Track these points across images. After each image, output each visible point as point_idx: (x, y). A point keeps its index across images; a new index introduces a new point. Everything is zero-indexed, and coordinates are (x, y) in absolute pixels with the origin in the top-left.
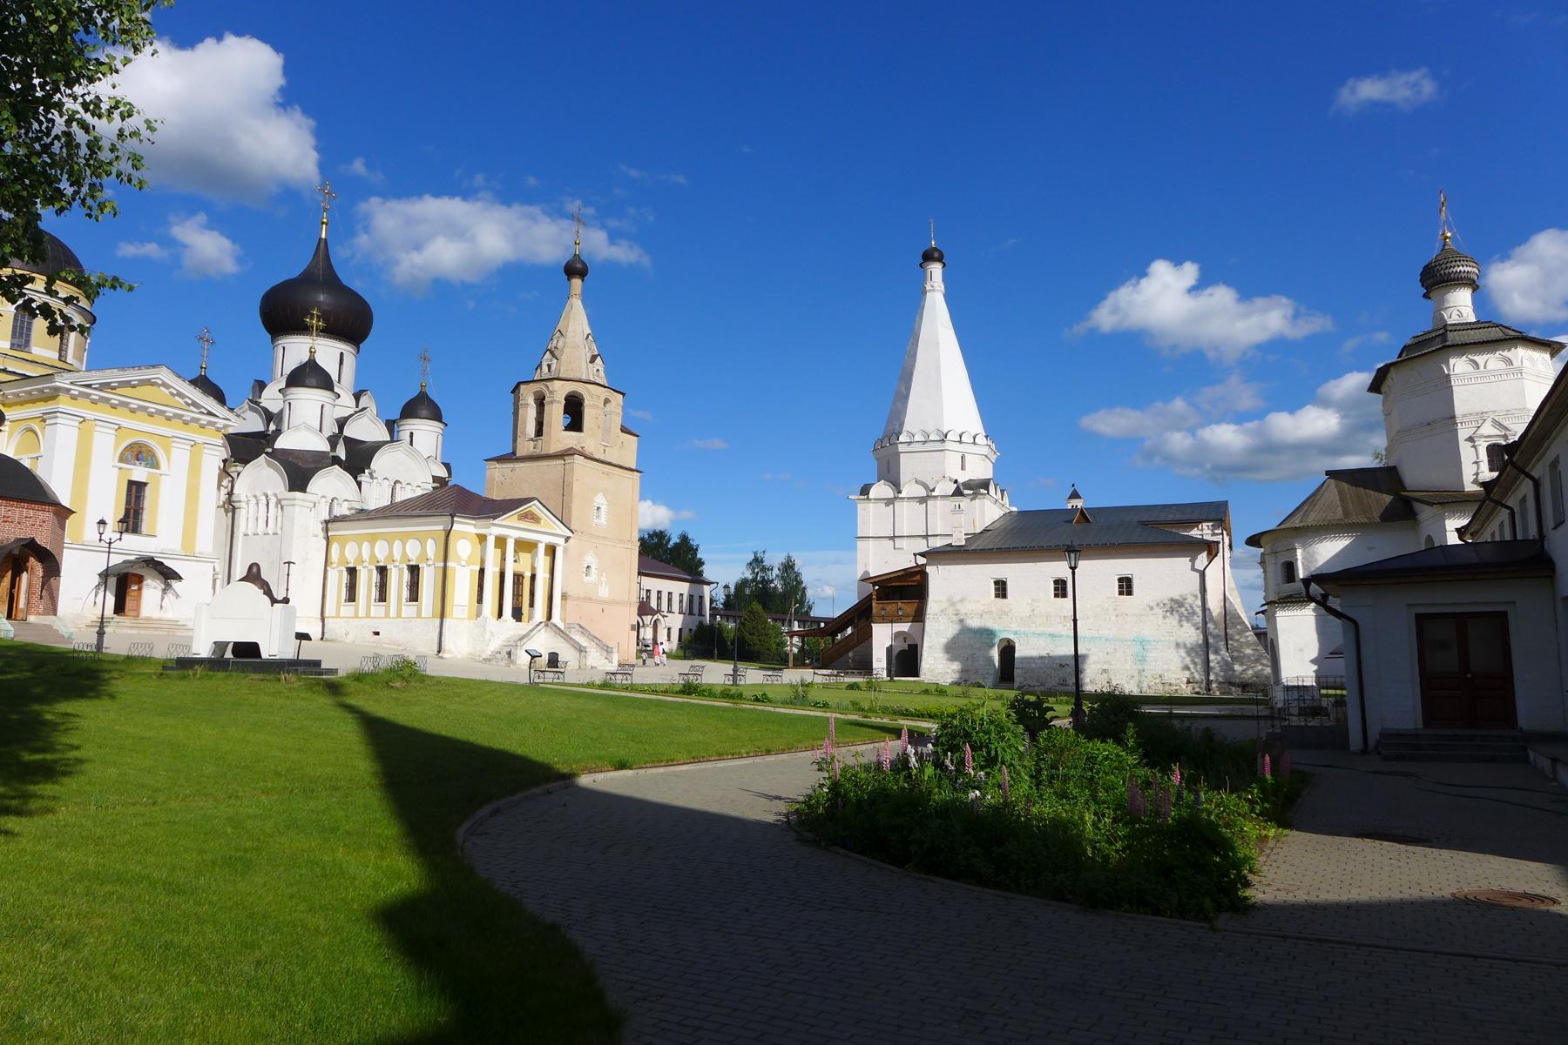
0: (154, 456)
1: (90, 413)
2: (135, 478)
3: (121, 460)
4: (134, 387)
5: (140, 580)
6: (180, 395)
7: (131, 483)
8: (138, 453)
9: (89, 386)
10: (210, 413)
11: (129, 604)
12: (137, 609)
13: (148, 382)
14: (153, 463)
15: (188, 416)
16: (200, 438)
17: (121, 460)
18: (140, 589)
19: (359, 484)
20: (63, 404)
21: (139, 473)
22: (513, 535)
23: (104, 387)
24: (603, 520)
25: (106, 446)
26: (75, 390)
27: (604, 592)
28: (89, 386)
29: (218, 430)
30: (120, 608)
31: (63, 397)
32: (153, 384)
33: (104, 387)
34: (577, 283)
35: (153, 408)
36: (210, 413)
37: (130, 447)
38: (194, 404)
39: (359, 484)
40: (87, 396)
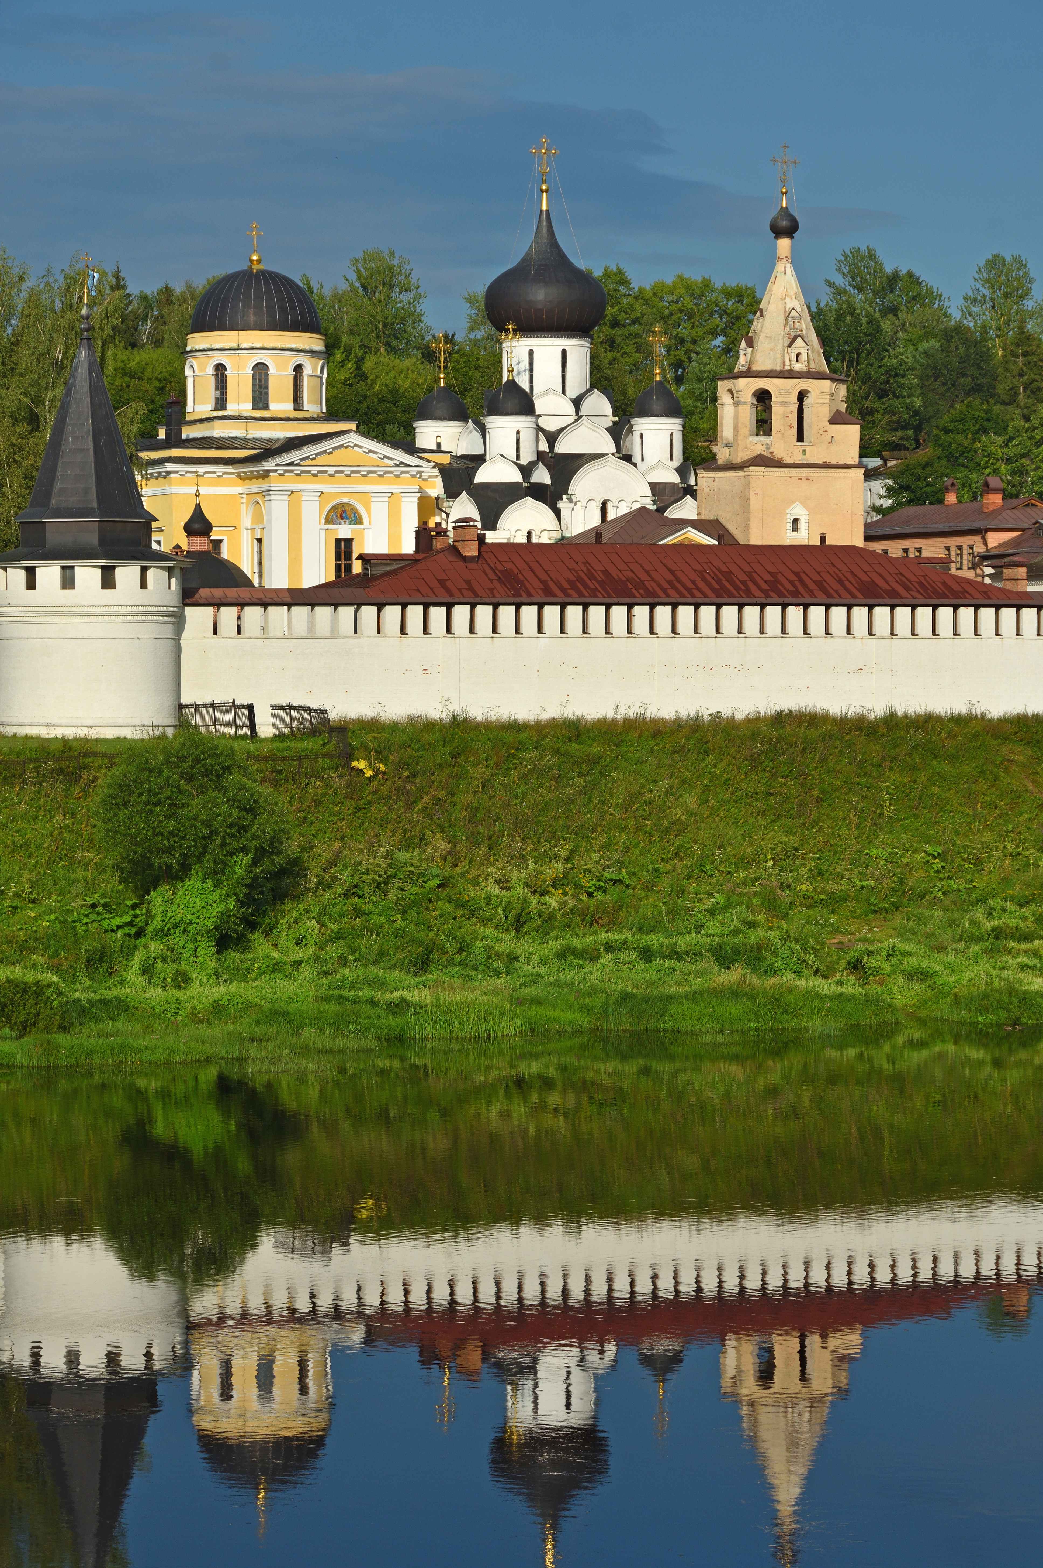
0: (356, 512)
3: (328, 521)
7: (338, 541)
8: (343, 513)
10: (402, 464)
13: (342, 446)
14: (357, 519)
16: (396, 489)
17: (328, 521)
19: (558, 513)
20: (274, 483)
21: (344, 531)
25: (312, 512)
34: (784, 244)
37: (335, 507)
39: (558, 513)
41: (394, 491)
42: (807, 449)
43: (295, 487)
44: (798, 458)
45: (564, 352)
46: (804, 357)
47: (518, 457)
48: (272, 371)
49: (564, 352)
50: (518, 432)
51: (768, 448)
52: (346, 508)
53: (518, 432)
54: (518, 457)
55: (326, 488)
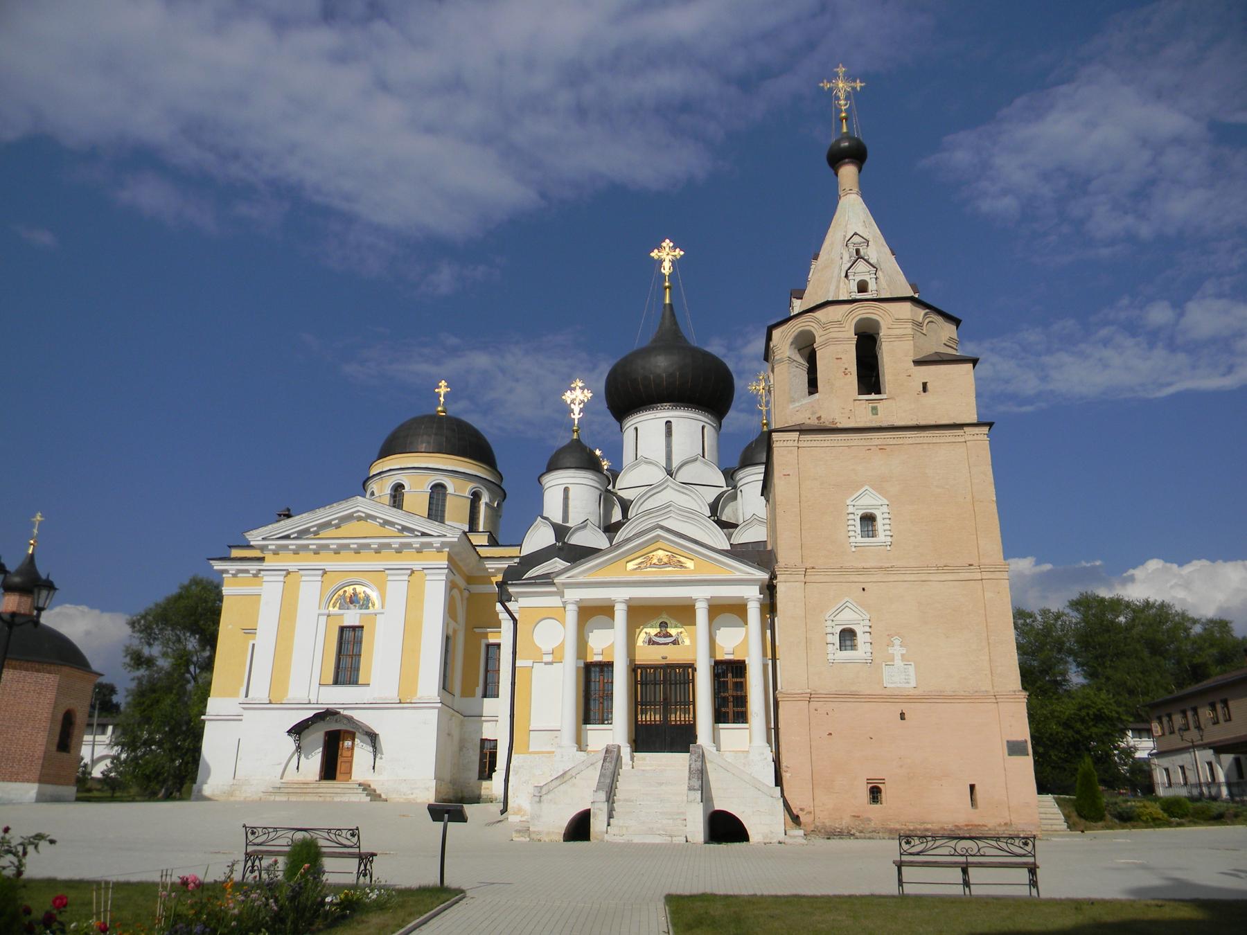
1: (292, 565)
2: (347, 622)
4: (338, 526)
5: (352, 736)
6: (386, 523)
7: (342, 629)
9: (287, 537)
10: (424, 534)
11: (341, 767)
12: (349, 772)
13: (349, 518)
15: (396, 542)
18: (352, 748)
21: (351, 617)
22: (620, 596)
23: (302, 534)
24: (882, 535)
26: (272, 545)
27: (900, 675)
28: (287, 537)
29: (439, 550)
30: (330, 770)
31: (268, 555)
32: (360, 519)
33: (302, 534)
35: (354, 543)
36: (424, 534)
38: (404, 529)
40: (286, 547)
41: (415, 568)
42: (880, 406)
43: (292, 565)
44: (864, 417)
45: (668, 423)
46: (872, 286)
47: (566, 517)
48: (407, 488)
49: (668, 423)
50: (566, 490)
51: (813, 413)
52: (359, 589)
53: (566, 490)
54: (566, 517)
55: (329, 566)
